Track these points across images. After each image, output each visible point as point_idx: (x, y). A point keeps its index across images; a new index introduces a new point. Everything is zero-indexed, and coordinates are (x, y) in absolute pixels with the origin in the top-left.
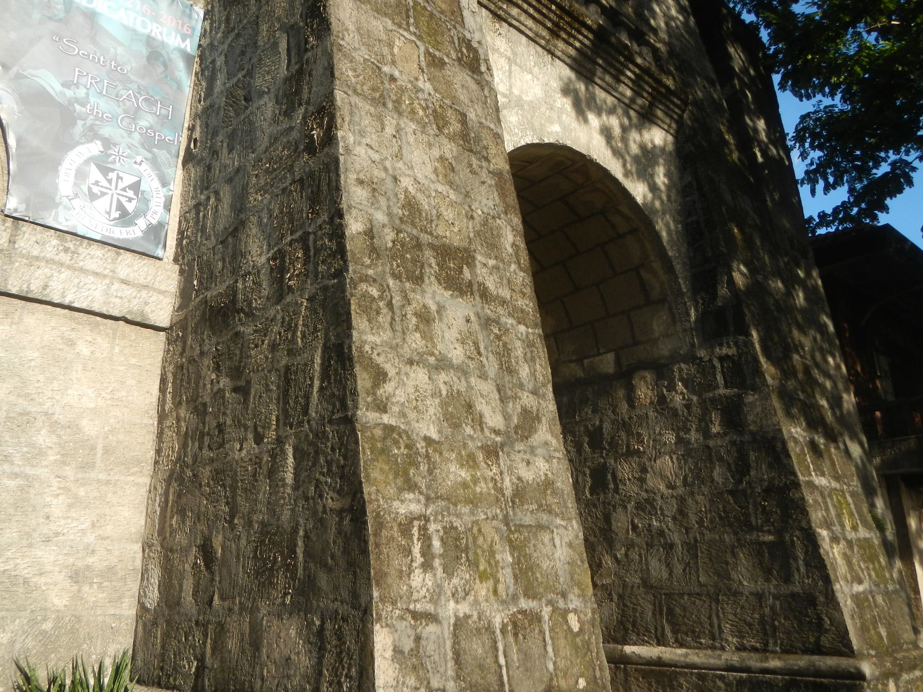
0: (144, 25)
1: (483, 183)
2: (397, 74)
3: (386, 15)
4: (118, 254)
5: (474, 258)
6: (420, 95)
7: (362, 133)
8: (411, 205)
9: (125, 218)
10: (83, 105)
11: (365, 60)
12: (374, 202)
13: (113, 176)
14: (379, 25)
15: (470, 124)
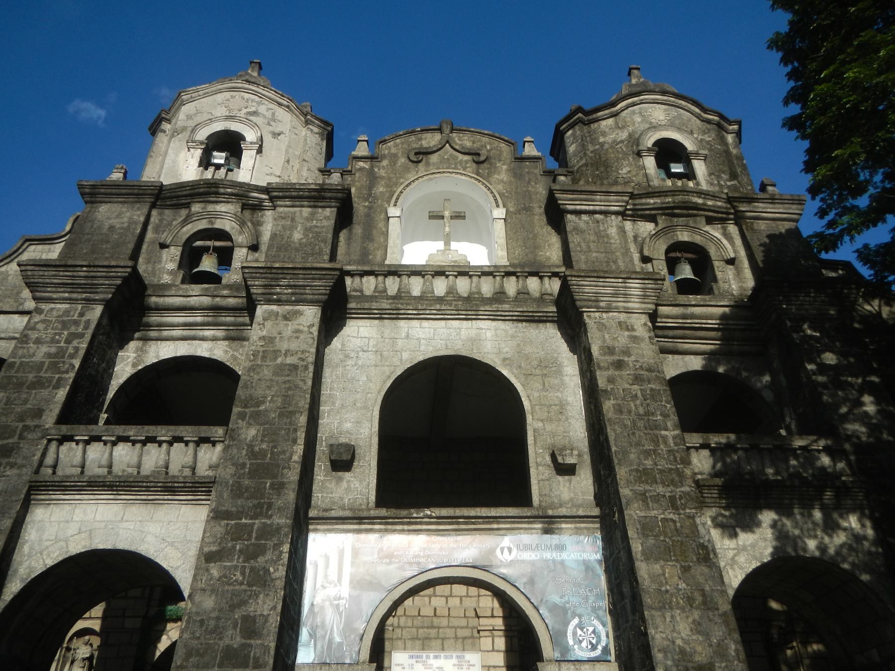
0: (581, 556)
1: (716, 623)
2: (668, 587)
3: (660, 559)
4: (594, 665)
5: (714, 666)
6: (680, 593)
7: (657, 628)
8: (682, 651)
9: (594, 647)
10: (568, 603)
11: (654, 589)
12: (666, 657)
13: (585, 630)
14: (657, 568)
15: (706, 593)
